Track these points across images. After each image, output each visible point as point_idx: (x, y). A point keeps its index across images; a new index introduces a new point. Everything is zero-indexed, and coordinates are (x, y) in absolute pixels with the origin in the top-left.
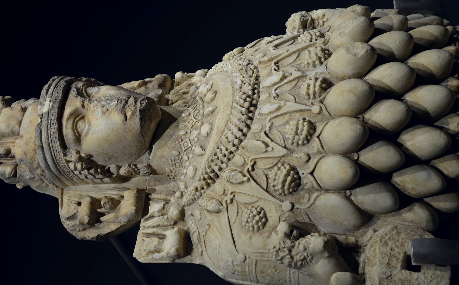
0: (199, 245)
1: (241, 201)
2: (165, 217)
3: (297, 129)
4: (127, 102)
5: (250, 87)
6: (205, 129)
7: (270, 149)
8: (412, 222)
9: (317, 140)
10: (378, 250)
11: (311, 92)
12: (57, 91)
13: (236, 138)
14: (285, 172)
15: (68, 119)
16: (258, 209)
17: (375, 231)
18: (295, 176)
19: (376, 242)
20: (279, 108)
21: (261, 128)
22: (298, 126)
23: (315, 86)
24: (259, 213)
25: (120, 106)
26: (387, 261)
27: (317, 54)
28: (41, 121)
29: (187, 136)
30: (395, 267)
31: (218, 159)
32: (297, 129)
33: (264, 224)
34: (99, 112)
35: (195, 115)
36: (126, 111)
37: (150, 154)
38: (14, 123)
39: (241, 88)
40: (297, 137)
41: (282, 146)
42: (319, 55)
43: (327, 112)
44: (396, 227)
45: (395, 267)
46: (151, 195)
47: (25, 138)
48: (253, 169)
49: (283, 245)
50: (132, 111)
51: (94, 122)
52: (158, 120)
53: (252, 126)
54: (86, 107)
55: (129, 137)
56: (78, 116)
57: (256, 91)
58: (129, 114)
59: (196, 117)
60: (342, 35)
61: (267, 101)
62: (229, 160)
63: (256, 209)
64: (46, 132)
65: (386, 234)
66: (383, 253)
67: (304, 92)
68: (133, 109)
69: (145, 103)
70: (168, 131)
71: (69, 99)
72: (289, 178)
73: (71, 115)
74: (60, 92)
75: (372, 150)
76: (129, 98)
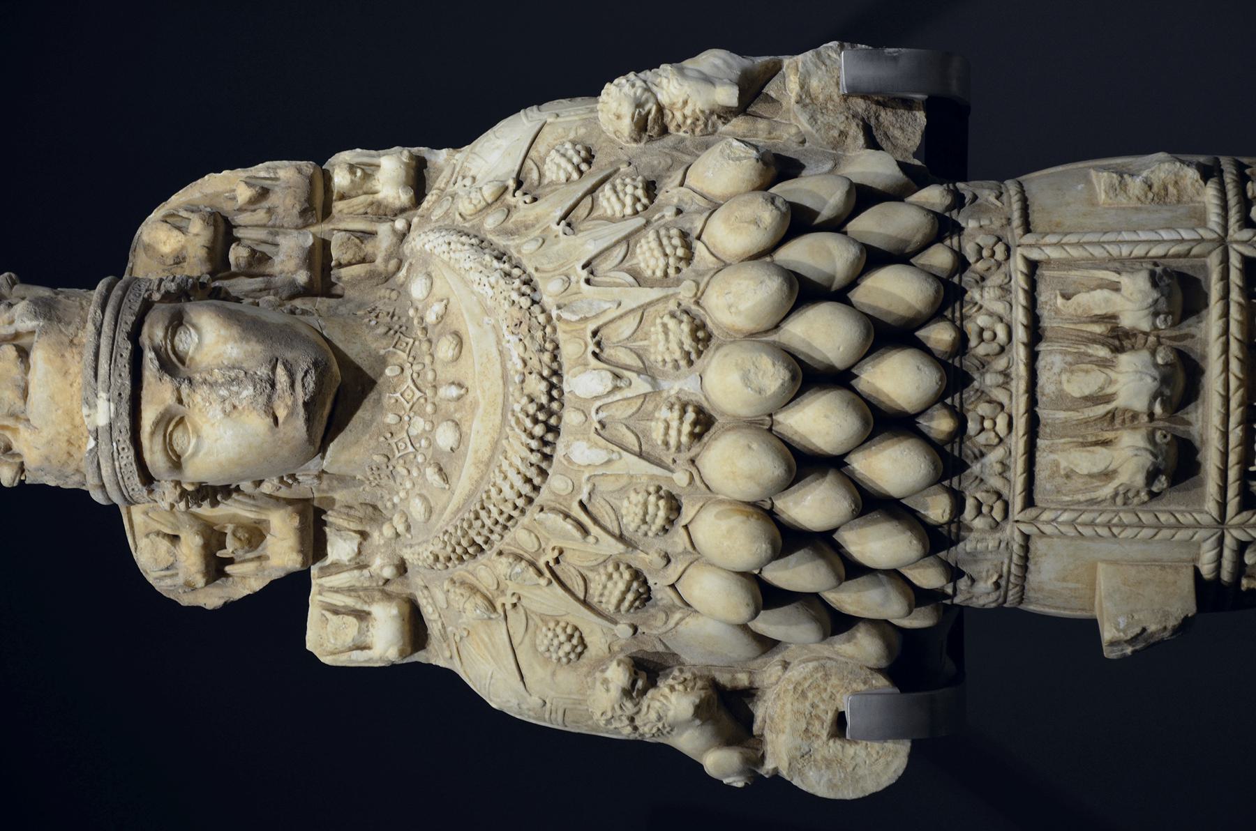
0: (445, 645)
1: (533, 608)
2: (366, 572)
3: (646, 513)
4: (273, 386)
5: (543, 386)
6: (445, 437)
7: (591, 539)
8: (852, 658)
9: (682, 532)
10: (789, 706)
11: (673, 442)
12: (117, 373)
13: (520, 495)
14: (621, 586)
15: (153, 434)
16: (569, 631)
17: (786, 665)
18: (641, 590)
19: (786, 691)
20: (609, 461)
21: (570, 488)
22: (646, 508)
23: (679, 432)
24: (570, 637)
25: (262, 400)
26: (804, 726)
27: (681, 344)
28: (97, 445)
29: (402, 427)
30: (817, 736)
31: (483, 526)
32: (646, 513)
33: (580, 655)
34: (215, 411)
35: (415, 375)
36: (275, 406)
37: (323, 458)
38: (11, 396)
39: (523, 381)
40: (644, 528)
41: (613, 535)
42: (687, 347)
43: (703, 486)
44: (823, 666)
45: (817, 736)
46: (325, 512)
47: (44, 434)
48: (557, 561)
49: (619, 712)
50: (287, 406)
51: (206, 430)
52: (335, 390)
53: (550, 471)
54: (185, 400)
55: (285, 452)
56: (171, 421)
57: (555, 393)
58: (282, 414)
59: (419, 382)
60: (733, 310)
61: (581, 433)
62: (505, 527)
63: (564, 629)
64: (110, 464)
65: (805, 678)
66: (798, 713)
67: (657, 436)
68: (290, 403)
69: (312, 385)
70: (359, 413)
71: (145, 384)
72: (630, 597)
73: (157, 424)
74: (126, 372)
75: (786, 568)
76: (274, 369)
